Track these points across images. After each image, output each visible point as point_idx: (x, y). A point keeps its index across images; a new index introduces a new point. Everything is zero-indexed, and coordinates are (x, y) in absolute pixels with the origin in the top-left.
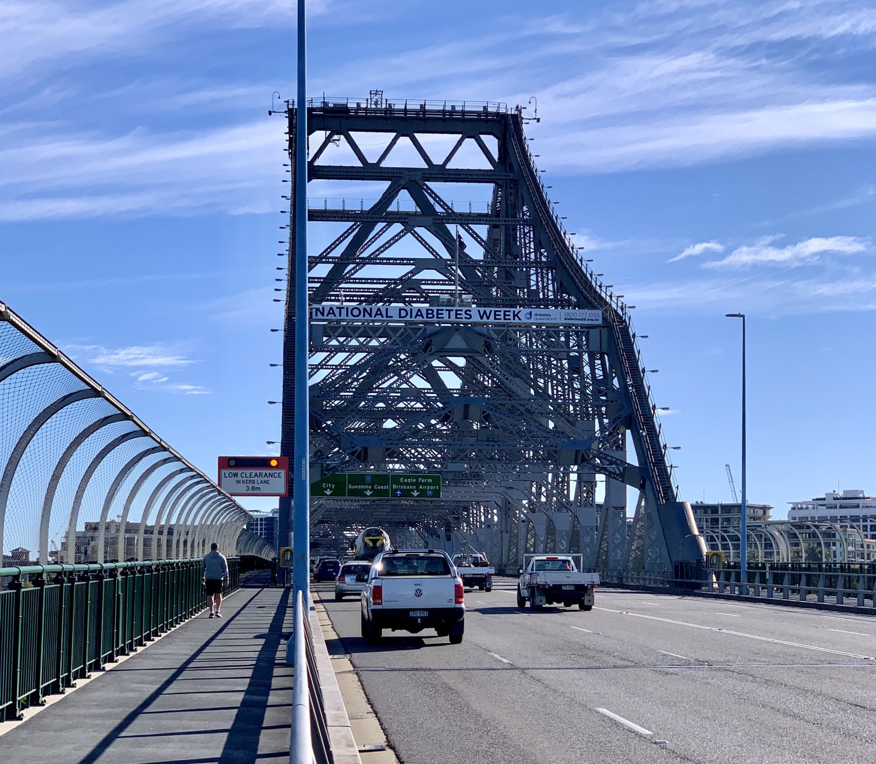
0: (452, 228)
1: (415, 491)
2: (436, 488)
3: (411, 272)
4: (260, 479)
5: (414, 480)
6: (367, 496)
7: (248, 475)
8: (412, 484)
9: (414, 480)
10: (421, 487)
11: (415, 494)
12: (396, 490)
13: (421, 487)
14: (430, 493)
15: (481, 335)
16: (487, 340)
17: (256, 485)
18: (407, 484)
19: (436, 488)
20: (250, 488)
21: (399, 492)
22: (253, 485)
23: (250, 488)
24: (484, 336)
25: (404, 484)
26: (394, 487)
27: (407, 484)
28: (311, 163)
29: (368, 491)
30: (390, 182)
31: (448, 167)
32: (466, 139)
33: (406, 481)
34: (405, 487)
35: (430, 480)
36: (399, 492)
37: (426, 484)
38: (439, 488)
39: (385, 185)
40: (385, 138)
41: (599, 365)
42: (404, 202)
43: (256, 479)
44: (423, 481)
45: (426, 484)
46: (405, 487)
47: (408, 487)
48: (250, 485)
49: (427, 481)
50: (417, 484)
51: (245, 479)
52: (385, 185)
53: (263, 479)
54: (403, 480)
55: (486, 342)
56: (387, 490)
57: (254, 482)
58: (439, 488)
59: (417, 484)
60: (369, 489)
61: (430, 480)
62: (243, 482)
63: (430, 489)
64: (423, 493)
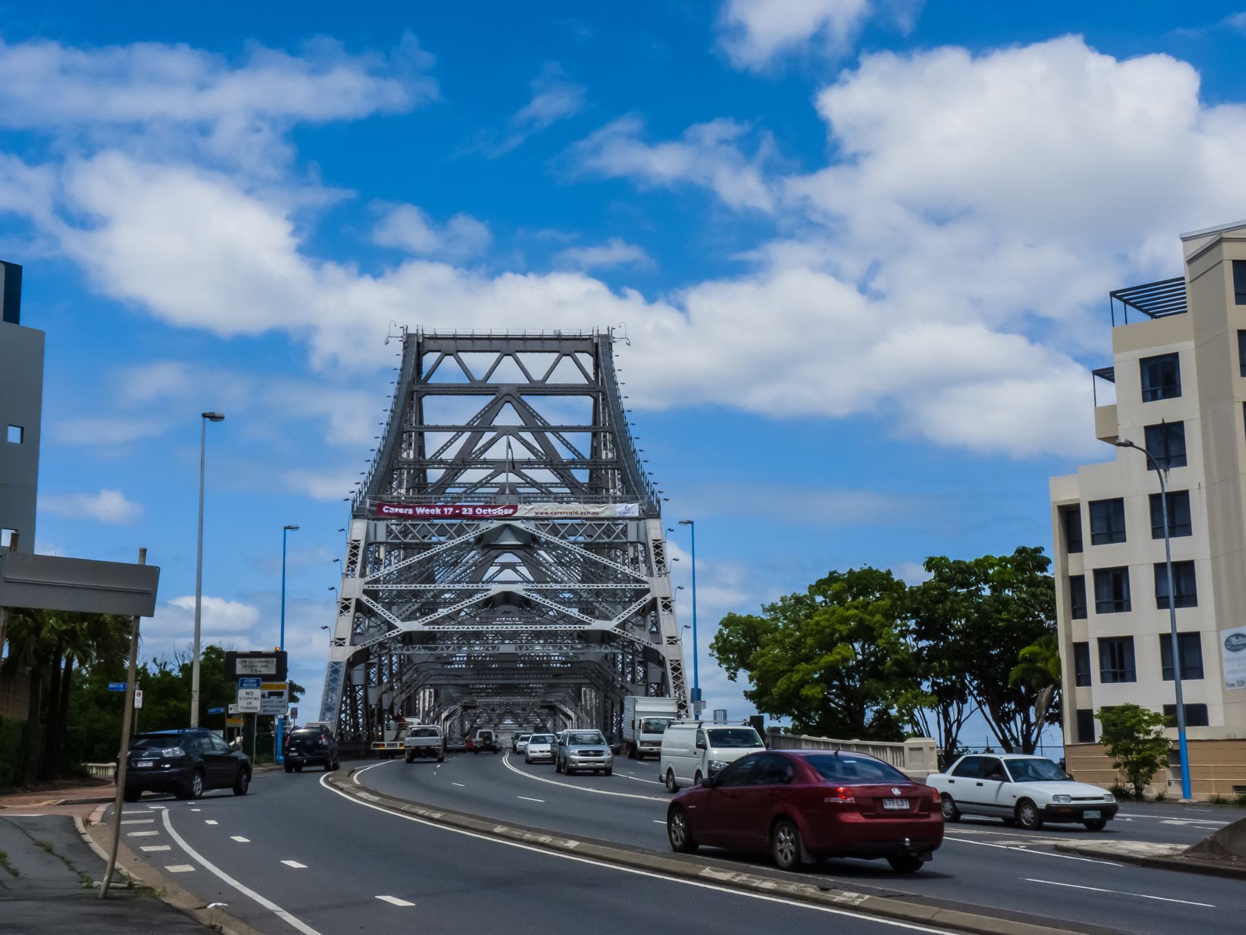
0: (549, 435)
3: (490, 475)
31: (490, 381)
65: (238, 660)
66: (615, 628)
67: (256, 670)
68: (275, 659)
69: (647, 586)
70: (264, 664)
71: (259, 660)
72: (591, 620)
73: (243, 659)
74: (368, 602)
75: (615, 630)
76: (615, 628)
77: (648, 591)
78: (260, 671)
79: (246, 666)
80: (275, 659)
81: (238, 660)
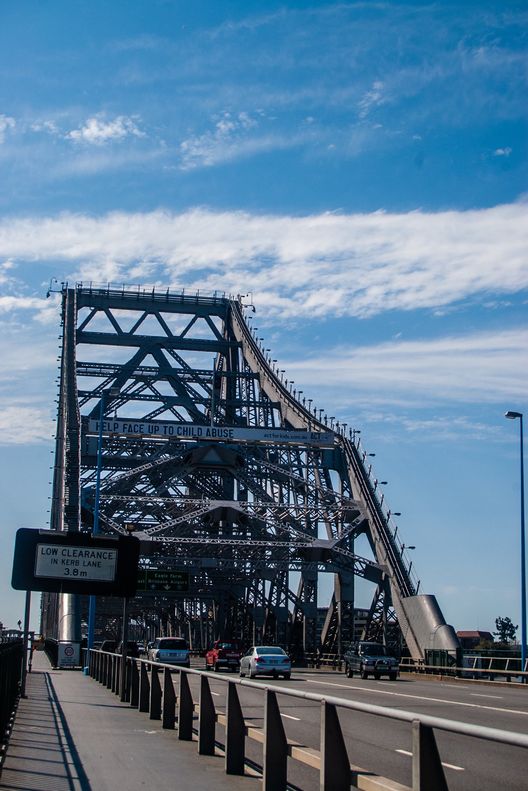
1: (167, 586)
2: (185, 583)
4: (87, 560)
5: (167, 576)
6: (165, 590)
7: (71, 553)
8: (165, 579)
9: (167, 576)
10: (172, 582)
11: (167, 587)
12: (151, 584)
13: (172, 582)
14: (180, 587)
15: (234, 450)
16: (239, 455)
17: (81, 568)
18: (160, 579)
19: (185, 583)
20: (71, 572)
21: (153, 586)
22: (76, 567)
23: (71, 572)
24: (236, 451)
26: (150, 581)
28: (79, 330)
30: (139, 348)
32: (199, 318)
33: (159, 576)
34: (158, 582)
35: (180, 576)
36: (153, 586)
38: (188, 583)
39: (135, 350)
40: (138, 314)
41: (324, 482)
42: (149, 361)
43: (81, 559)
44: (174, 577)
46: (158, 582)
47: (161, 582)
48: (71, 568)
49: (177, 577)
50: (169, 579)
51: (67, 558)
52: (135, 350)
53: (92, 559)
54: (158, 575)
55: (238, 456)
56: (143, 585)
57: (77, 563)
58: (188, 583)
59: (169, 579)
61: (180, 576)
62: (63, 561)
63: (180, 584)
64: (174, 587)
65: (41, 548)
66: (336, 547)
67: (76, 571)
68: (114, 553)
69: (356, 509)
70: (92, 559)
71: (84, 550)
72: (311, 539)
73: (51, 547)
75: (337, 549)
76: (336, 547)
77: (358, 513)
78: (83, 573)
79: (56, 561)
80: (114, 553)
81: (41, 548)
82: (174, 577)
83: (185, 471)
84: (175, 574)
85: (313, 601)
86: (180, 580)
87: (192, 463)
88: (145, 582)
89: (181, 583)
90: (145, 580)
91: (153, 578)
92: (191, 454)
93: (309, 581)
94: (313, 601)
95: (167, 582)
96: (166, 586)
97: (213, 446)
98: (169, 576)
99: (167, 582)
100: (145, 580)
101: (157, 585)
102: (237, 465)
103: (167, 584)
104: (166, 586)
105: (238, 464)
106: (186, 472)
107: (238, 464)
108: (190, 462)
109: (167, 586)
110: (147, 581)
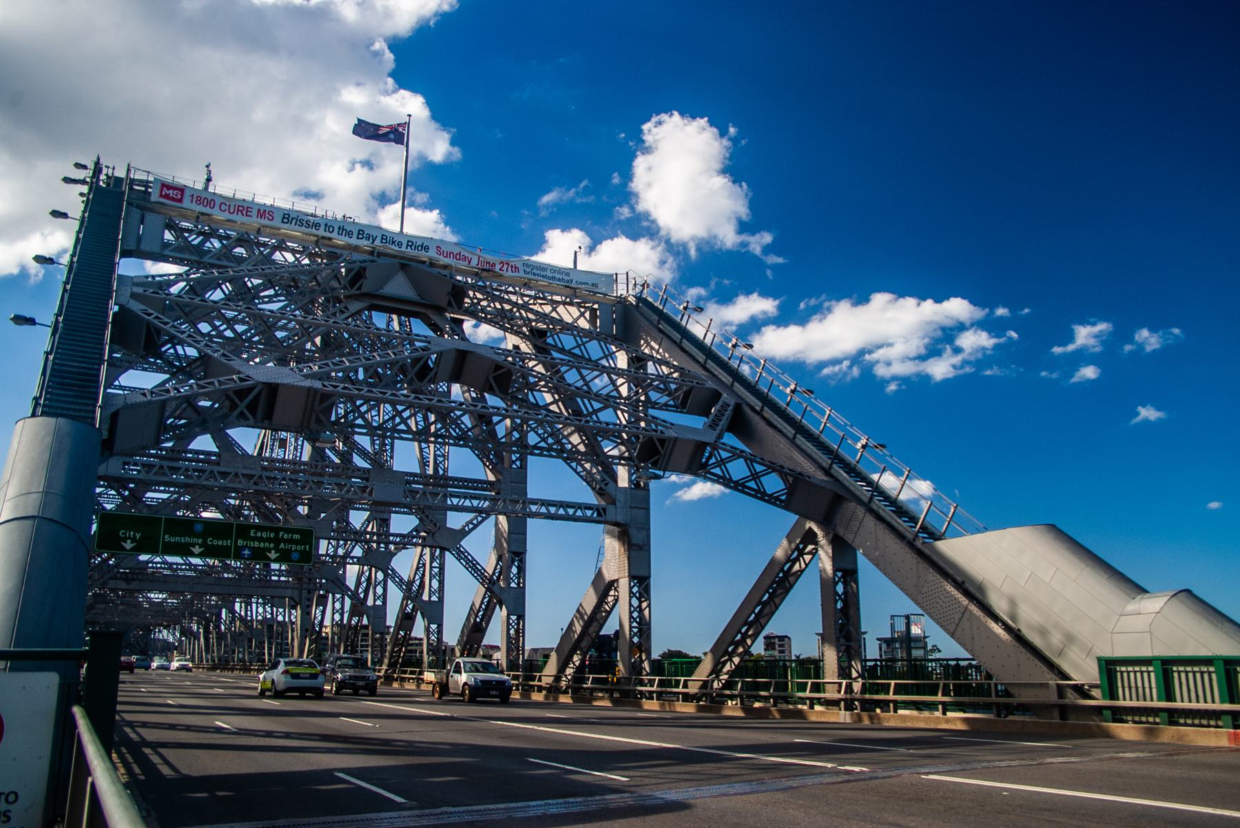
1: (273, 552)
2: (305, 548)
8: (269, 540)
9: (272, 535)
10: (282, 546)
13: (282, 546)
14: (295, 556)
18: (260, 540)
19: (305, 548)
21: (247, 552)
25: (254, 539)
26: (240, 542)
27: (260, 540)
29: (197, 547)
33: (259, 534)
35: (296, 536)
36: (247, 552)
37: (291, 541)
44: (286, 536)
45: (291, 541)
47: (262, 545)
49: (292, 537)
54: (255, 533)
59: (277, 541)
60: (198, 544)
61: (296, 536)
63: (296, 550)
74: (150, 315)
82: (286, 536)
83: (346, 308)
84: (288, 531)
85: (437, 600)
86: (297, 542)
87: (364, 290)
88: (231, 543)
89: (299, 548)
90: (231, 540)
91: (246, 537)
92: (365, 269)
93: (513, 553)
94: (437, 600)
95: (272, 545)
96: (270, 553)
97: (403, 267)
98: (277, 534)
99: (272, 545)
100: (231, 540)
101: (253, 549)
102: (450, 304)
103: (273, 549)
104: (270, 553)
105: (452, 300)
106: (347, 309)
107: (452, 300)
108: (359, 288)
109: (273, 552)
110: (236, 542)
